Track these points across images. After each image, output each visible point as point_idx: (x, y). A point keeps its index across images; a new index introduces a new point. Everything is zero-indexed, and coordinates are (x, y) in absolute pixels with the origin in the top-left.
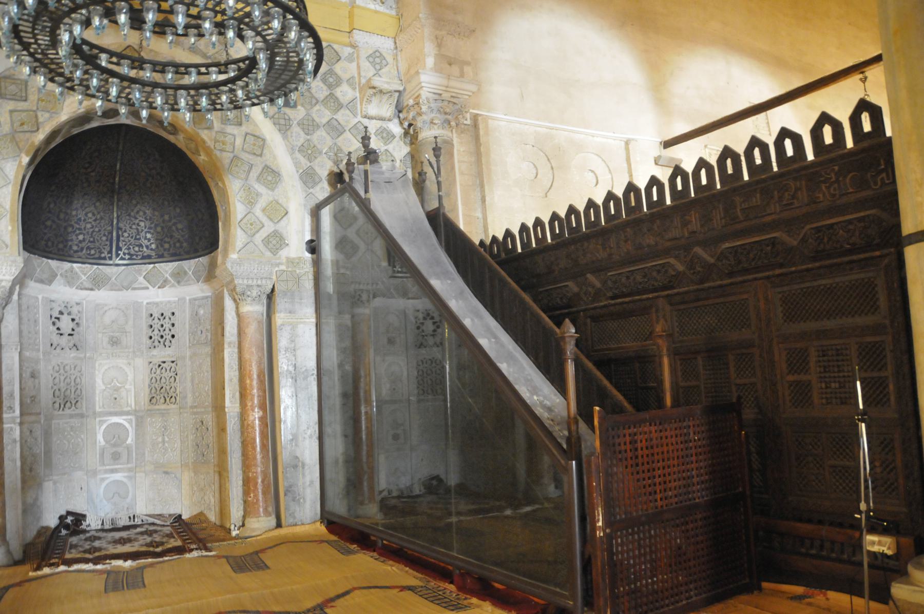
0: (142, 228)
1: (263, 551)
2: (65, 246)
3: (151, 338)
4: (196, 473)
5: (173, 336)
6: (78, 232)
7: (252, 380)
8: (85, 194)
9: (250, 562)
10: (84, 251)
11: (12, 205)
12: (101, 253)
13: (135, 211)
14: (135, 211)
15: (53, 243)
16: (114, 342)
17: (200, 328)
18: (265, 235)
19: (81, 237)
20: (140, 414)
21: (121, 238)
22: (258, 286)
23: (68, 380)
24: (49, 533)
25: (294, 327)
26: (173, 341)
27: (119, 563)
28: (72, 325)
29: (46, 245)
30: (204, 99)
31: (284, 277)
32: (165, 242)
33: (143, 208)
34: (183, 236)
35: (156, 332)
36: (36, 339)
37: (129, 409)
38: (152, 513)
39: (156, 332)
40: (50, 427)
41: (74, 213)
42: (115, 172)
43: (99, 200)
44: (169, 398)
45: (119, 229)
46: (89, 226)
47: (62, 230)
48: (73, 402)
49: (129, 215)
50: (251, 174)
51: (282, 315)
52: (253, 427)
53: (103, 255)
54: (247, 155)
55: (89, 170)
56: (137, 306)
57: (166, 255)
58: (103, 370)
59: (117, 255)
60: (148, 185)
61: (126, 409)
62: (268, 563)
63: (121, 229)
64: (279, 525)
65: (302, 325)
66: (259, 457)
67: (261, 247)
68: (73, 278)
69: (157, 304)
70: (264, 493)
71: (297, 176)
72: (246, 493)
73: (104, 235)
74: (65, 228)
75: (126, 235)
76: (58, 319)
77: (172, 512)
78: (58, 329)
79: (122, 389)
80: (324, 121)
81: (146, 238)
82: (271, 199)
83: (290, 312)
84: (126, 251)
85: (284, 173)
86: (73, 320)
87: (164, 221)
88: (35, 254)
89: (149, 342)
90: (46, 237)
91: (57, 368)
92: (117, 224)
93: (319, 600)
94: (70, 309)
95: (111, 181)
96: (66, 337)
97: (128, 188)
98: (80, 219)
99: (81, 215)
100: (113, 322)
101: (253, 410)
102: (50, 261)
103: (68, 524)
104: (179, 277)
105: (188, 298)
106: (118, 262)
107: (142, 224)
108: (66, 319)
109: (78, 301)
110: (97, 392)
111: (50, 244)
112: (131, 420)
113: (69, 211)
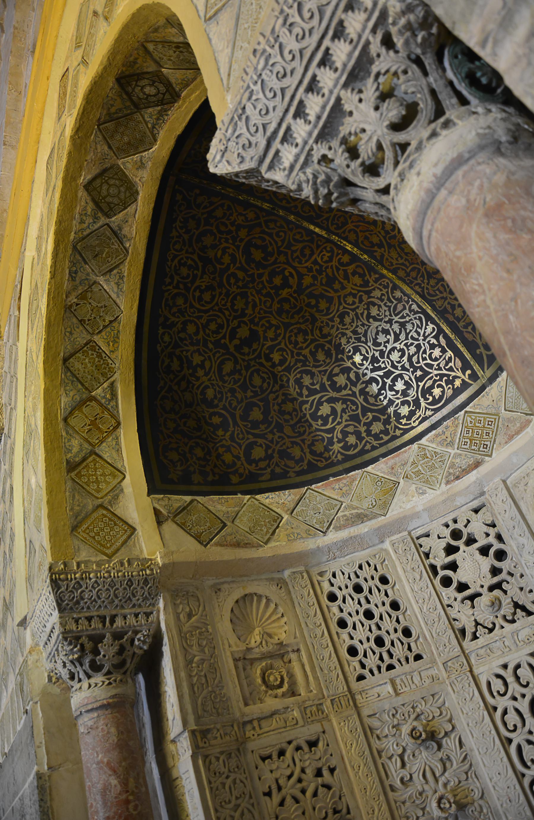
2: (387, 422)
6: (389, 381)
10: (423, 404)
15: (358, 434)
19: (400, 386)
29: (347, 447)
42: (328, 241)
53: (458, 383)
55: (293, 282)
63: (445, 311)
74: (363, 392)
78: (462, 587)
88: (326, 478)
92: (434, 308)
95: (346, 259)
98: (374, 360)
102: (369, 468)
106: (489, 373)
109: (475, 504)
111: (352, 440)
113: (349, 364)
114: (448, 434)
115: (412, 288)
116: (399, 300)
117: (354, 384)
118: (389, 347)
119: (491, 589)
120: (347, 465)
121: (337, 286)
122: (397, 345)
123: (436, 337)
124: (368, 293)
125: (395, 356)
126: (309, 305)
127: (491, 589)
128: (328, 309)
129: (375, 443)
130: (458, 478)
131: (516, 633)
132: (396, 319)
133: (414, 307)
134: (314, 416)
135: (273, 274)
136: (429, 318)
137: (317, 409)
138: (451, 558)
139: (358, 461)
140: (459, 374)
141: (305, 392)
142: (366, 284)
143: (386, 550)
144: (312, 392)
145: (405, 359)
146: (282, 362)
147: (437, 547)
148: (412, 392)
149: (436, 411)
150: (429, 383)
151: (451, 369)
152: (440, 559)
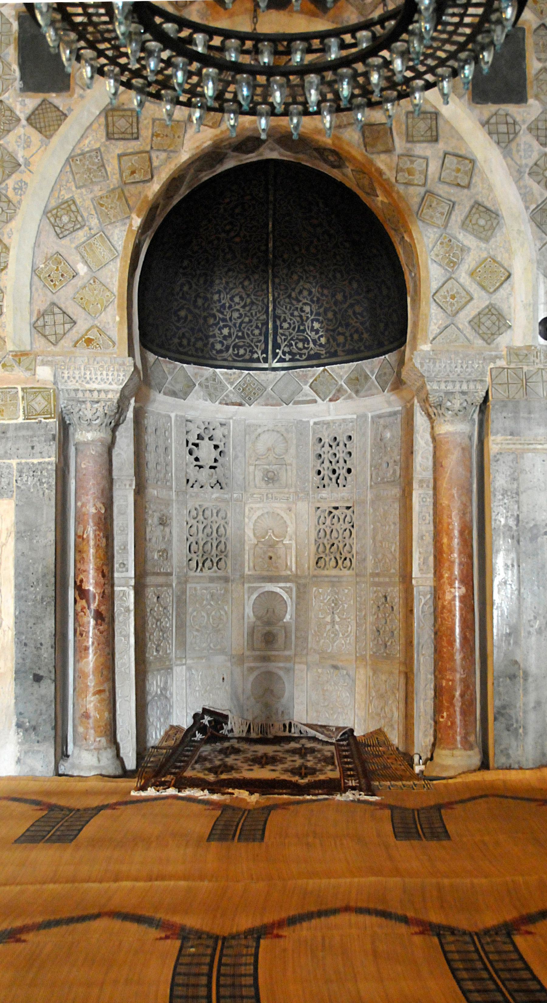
0: (308, 314)
1: (450, 805)
2: (205, 345)
3: (319, 473)
4: (375, 672)
5: (349, 471)
7: (451, 539)
8: (229, 270)
9: (422, 823)
10: (231, 350)
11: (120, 287)
12: (252, 352)
13: (297, 290)
14: (297, 290)
17: (386, 459)
18: (474, 313)
19: (226, 331)
20: (302, 581)
21: (280, 331)
22: (463, 393)
23: (208, 530)
24: (180, 736)
25: (517, 456)
26: (349, 477)
27: (243, 794)
28: (214, 454)
29: (181, 345)
30: (345, 86)
31: (503, 378)
32: (339, 334)
33: (307, 286)
34: (362, 324)
36: (167, 472)
37: (289, 573)
38: (315, 722)
39: (327, 464)
40: (184, 592)
41: (216, 297)
42: (268, 234)
43: (247, 278)
44: (342, 559)
45: (276, 317)
46: (236, 315)
47: (201, 321)
48: (215, 560)
49: (289, 296)
50: (453, 217)
52: (451, 611)
53: (255, 356)
54: (446, 188)
55: (232, 234)
56: (300, 427)
57: (340, 353)
58: (254, 518)
59: (275, 355)
60: (313, 250)
61: (283, 573)
62: (450, 828)
63: (279, 318)
64: (485, 765)
65: (530, 454)
66: (458, 657)
67: (468, 331)
68: (216, 389)
69: (328, 424)
70: (464, 713)
71: (526, 216)
72: (438, 710)
73: (257, 327)
74: (205, 318)
75: (286, 325)
76: (197, 445)
77: (341, 725)
78: (197, 459)
79: (280, 545)
81: (312, 329)
82: (485, 255)
83: (512, 434)
84: (287, 349)
85: (504, 212)
86: (216, 447)
87: (336, 303)
88: (164, 357)
89: (317, 478)
90: (180, 332)
91: (194, 513)
92: (274, 309)
93: (510, 915)
94: (212, 433)
95: (263, 248)
96: (206, 471)
97: (286, 256)
98: (223, 306)
99: (226, 301)
100: (269, 450)
101: (452, 585)
102: (185, 365)
103: (205, 726)
104: (358, 384)
105: (370, 415)
106: (276, 365)
107: (307, 309)
108: (206, 446)
109: (223, 421)
110: (247, 548)
111: (185, 342)
112: (291, 589)
113: (209, 296)
114: (233, 377)
115: (273, 291)
116: (263, 290)
117: (205, 310)
118: (237, 307)
119: (211, 467)
120: (177, 356)
121: (244, 255)
122: (241, 310)
123: (263, 324)
124: (253, 272)
125: (236, 315)
126: (223, 251)
127: (211, 467)
128: (228, 260)
129: (194, 353)
130: (227, 404)
131: (212, 494)
132: (253, 297)
133: (266, 300)
134: (176, 313)
135: (231, 223)
136: (267, 312)
137: (179, 310)
138: (197, 441)
139: (183, 357)
140: (260, 352)
141: (181, 295)
142: (257, 267)
143: (170, 417)
144: (183, 298)
145: (239, 321)
146: (185, 268)
148: (229, 341)
149: (235, 361)
150: (241, 344)
151: (257, 346)
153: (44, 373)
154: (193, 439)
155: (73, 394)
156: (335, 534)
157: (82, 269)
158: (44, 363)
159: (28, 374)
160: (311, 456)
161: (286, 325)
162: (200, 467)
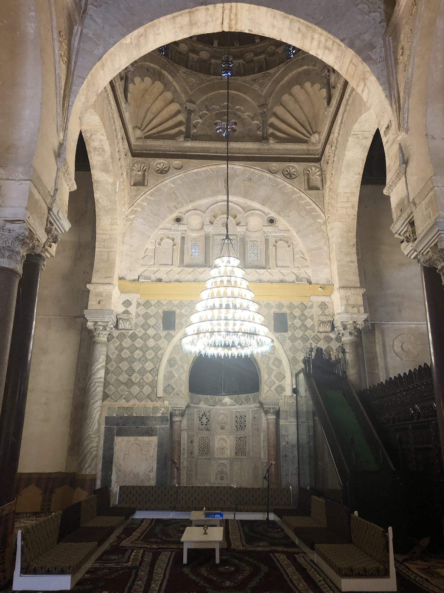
3: (236, 426)
16: (222, 428)
22: (273, 408)
23: (204, 444)
35: (239, 424)
39: (239, 424)
51: (283, 420)
67: (274, 391)
78: (202, 422)
80: (300, 336)
82: (278, 371)
86: (207, 419)
91: (200, 438)
96: (204, 426)
104: (247, 400)
147: (201, 414)
152: (201, 416)
153: (166, 403)
154: (201, 416)
155: (173, 408)
156: (241, 445)
157: (176, 375)
158: (166, 400)
159: (162, 403)
160: (234, 422)
161: (227, 383)
162: (202, 424)
